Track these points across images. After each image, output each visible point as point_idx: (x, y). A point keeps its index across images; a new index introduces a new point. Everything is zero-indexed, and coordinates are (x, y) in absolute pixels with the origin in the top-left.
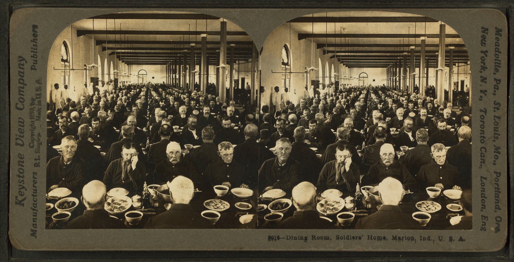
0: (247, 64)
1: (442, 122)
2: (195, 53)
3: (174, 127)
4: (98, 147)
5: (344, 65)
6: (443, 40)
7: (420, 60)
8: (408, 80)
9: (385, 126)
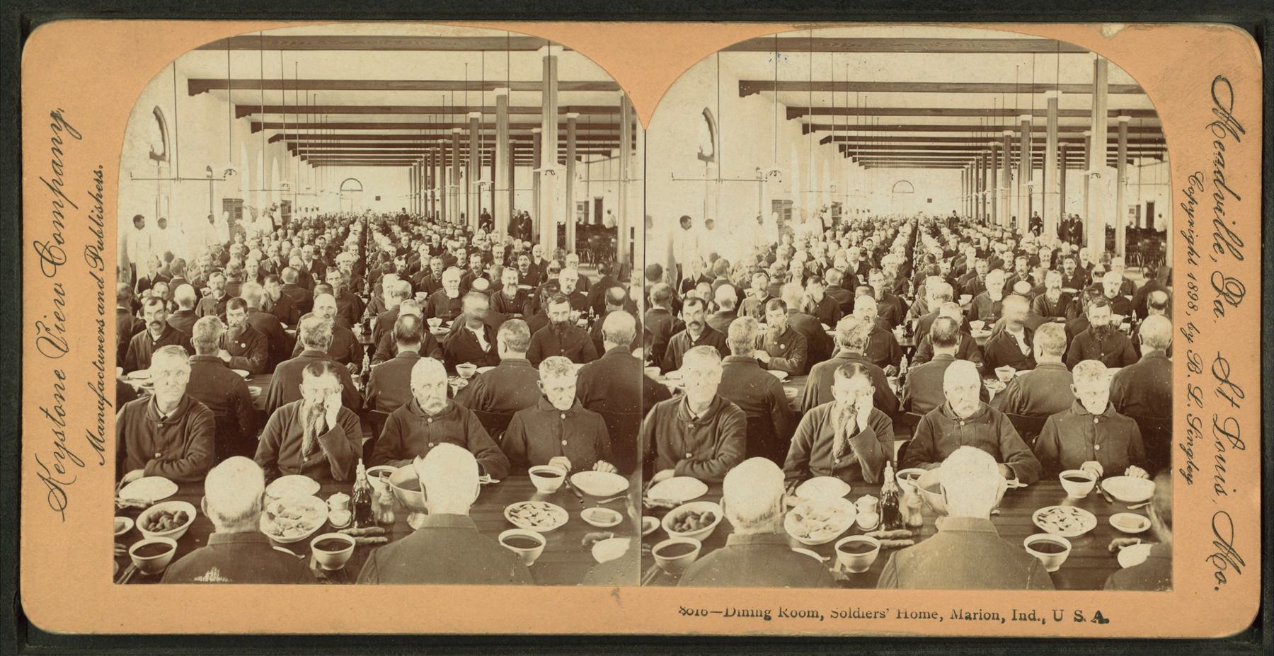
0: (607, 162)
1: (1100, 305)
2: (480, 137)
3: (430, 321)
4: (244, 373)
5: (854, 160)
6: (1101, 99)
7: (1044, 148)
8: (1014, 199)
9: (958, 317)
